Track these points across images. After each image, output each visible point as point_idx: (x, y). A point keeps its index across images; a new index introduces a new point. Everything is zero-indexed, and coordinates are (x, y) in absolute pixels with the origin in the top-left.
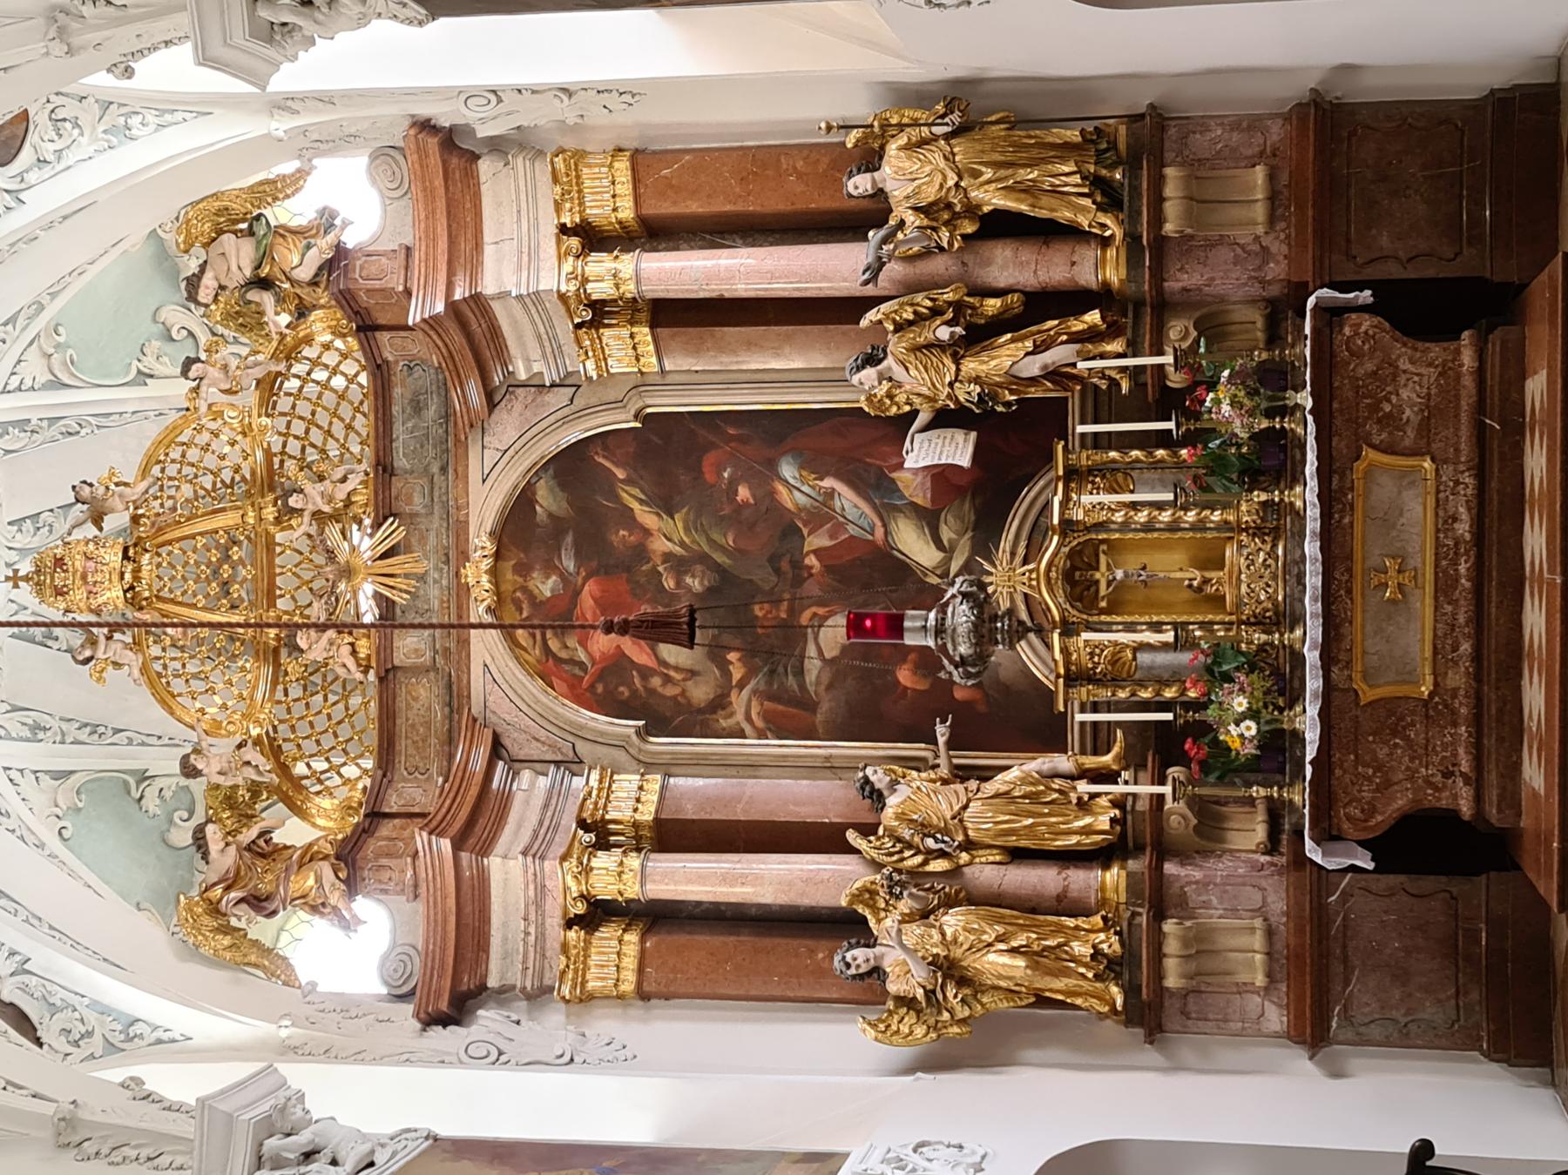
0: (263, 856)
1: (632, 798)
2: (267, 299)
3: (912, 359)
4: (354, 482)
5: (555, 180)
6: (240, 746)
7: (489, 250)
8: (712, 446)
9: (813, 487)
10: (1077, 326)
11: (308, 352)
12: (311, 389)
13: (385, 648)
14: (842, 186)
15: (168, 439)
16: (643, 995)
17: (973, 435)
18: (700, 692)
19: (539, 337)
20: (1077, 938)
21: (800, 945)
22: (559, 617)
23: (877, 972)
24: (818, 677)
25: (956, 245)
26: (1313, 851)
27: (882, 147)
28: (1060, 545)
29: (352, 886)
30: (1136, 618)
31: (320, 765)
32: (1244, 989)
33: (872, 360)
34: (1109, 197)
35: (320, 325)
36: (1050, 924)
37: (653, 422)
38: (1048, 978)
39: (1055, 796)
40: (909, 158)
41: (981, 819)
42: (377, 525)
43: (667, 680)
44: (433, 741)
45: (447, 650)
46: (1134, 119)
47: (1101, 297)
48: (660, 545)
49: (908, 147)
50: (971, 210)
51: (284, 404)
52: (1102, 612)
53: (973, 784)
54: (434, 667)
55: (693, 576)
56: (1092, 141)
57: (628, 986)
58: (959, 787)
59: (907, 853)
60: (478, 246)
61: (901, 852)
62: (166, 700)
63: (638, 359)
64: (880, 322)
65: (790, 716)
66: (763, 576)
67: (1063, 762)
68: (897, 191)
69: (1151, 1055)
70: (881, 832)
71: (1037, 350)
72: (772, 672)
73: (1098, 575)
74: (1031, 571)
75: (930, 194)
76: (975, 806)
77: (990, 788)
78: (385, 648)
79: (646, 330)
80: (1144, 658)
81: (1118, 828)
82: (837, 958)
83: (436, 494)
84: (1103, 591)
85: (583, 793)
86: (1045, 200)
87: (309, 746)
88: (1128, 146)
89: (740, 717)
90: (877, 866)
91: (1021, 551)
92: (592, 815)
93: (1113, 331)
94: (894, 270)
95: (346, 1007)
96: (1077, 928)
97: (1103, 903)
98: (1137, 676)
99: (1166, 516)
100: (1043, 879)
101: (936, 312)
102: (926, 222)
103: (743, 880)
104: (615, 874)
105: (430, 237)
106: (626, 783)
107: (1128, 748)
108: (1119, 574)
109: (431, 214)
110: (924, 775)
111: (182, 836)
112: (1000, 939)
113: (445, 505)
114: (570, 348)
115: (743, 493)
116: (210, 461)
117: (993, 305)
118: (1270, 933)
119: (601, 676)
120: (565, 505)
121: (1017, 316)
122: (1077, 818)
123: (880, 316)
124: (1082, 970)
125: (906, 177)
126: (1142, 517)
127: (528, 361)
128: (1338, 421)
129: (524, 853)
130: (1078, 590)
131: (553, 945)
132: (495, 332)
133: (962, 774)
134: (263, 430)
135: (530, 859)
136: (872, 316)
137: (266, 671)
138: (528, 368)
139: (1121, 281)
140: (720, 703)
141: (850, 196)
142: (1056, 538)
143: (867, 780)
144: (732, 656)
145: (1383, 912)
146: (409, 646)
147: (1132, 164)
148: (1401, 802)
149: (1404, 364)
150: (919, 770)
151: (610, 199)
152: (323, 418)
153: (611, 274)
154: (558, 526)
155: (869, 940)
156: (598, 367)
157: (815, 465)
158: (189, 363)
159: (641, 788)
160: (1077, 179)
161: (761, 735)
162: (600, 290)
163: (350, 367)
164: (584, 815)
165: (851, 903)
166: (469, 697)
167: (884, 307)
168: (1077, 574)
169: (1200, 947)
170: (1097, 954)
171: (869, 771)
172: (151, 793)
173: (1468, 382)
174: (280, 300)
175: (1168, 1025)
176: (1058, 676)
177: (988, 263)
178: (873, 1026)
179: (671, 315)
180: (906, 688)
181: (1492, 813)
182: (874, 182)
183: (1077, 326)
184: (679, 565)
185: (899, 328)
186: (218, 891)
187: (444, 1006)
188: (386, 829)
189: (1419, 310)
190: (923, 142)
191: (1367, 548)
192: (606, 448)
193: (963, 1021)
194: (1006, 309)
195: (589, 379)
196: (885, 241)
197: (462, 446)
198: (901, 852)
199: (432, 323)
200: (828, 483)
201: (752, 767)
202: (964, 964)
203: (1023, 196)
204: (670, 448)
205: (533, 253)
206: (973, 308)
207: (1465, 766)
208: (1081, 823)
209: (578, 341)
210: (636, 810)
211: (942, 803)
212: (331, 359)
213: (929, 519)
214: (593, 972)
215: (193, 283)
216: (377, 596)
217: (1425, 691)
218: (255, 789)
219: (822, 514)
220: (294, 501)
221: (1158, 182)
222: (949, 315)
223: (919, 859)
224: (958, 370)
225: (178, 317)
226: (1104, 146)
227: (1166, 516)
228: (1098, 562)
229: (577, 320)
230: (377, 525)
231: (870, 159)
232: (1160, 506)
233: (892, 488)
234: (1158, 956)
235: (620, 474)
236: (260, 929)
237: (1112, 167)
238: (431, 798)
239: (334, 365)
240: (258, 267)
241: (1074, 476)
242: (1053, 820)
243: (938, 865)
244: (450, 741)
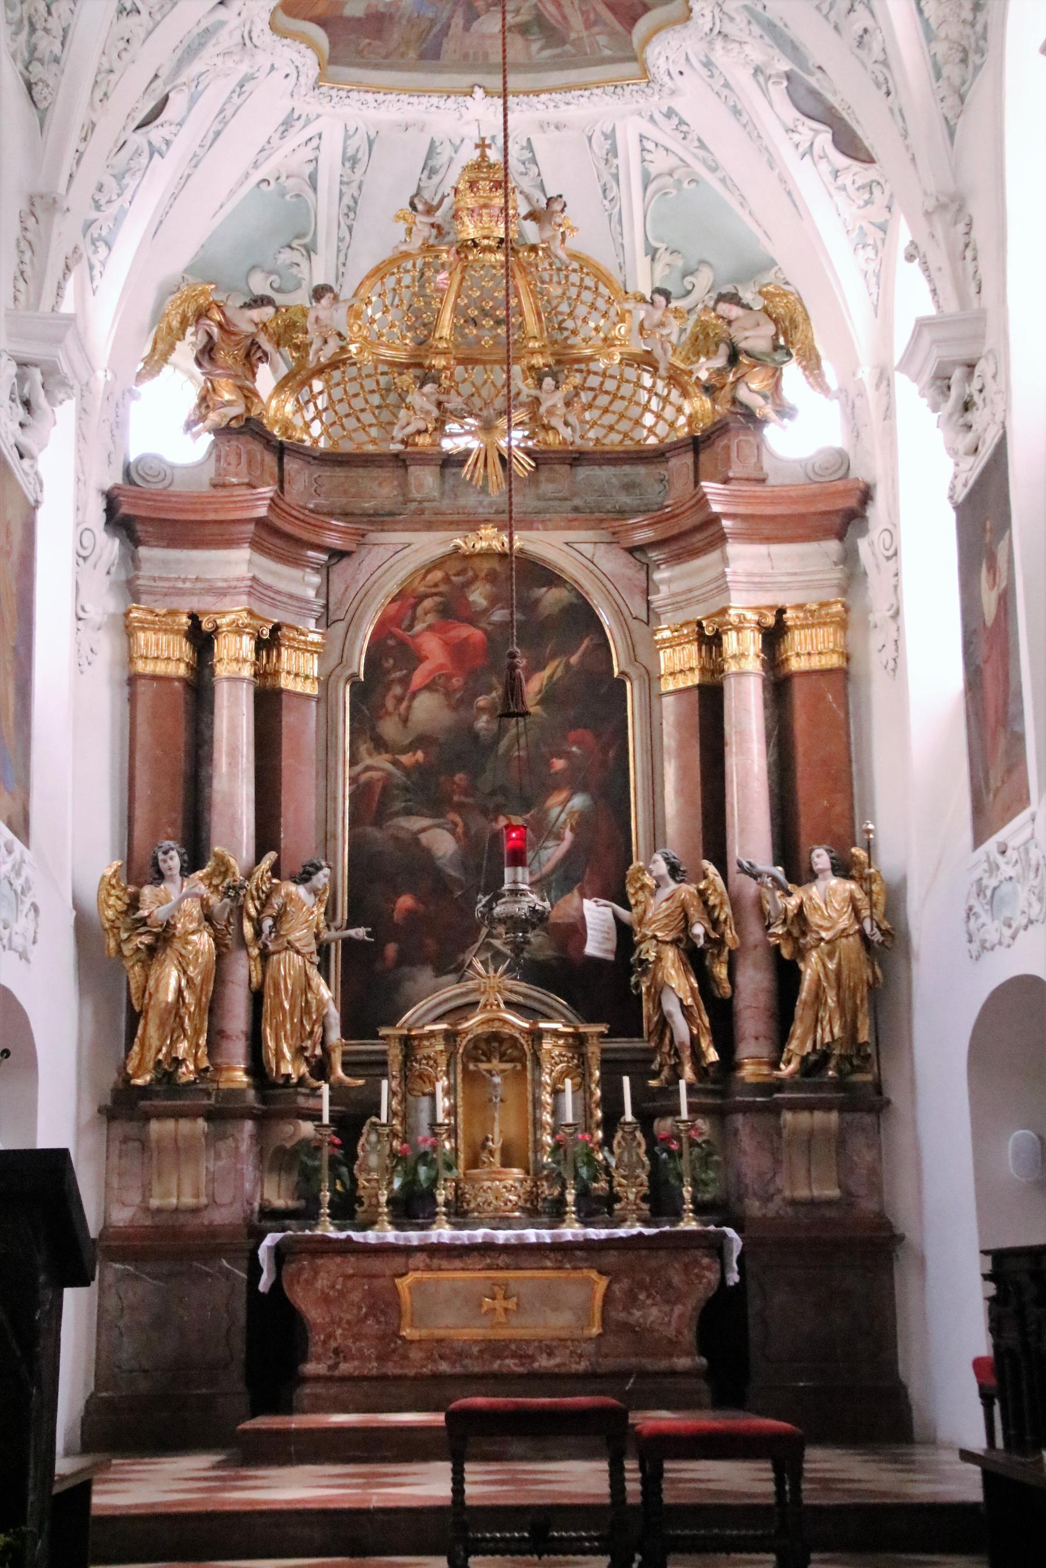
0: (248, 355)
1: (299, 671)
2: (720, 361)
3: (675, 904)
4: (566, 433)
5: (822, 605)
6: (340, 335)
7: (762, 549)
8: (598, 736)
9: (565, 822)
10: (705, 1042)
11: (675, 395)
12: (644, 396)
14: (819, 844)
15: (601, 276)
16: (133, 680)
17: (611, 957)
18: (389, 728)
19: (690, 590)
20: (190, 1047)
21: (178, 817)
22: (452, 610)
23: (159, 877)
24: (402, 828)
25: (772, 939)
26: (270, 1240)
27: (852, 878)
28: (522, 1030)
29: (223, 432)
30: (460, 1094)
31: (321, 402)
32: (146, 1191)
33: (674, 870)
34: (813, 1066)
35: (699, 404)
36: (202, 1023)
37: (619, 687)
38: (157, 1021)
39: (308, 1028)
40: (844, 900)
41: (289, 966)
42: (528, 452)
43: (399, 700)
44: (344, 500)
45: (422, 512)
46: (878, 1087)
47: (729, 1062)
49: (852, 900)
50: (801, 952)
51: (631, 373)
52: (465, 1069)
53: (316, 959)
54: (407, 501)
55: (488, 722)
56: (859, 1051)
57: (141, 667)
58: (314, 947)
59: (257, 903)
60: (768, 540)
61: (259, 898)
62: (379, 272)
63: (672, 674)
64: (706, 877)
65: (370, 805)
66: (487, 781)
67: (335, 1035)
68: (815, 891)
69: (90, 1110)
70: (275, 881)
71: (685, 1009)
72: (406, 789)
73: (495, 1061)
74: (498, 1005)
75: (814, 919)
76: (298, 960)
77: (313, 972)
78: (423, 459)
79: (696, 681)
80: (425, 1102)
81: (281, 1081)
82: (171, 843)
83: (556, 503)
84: (483, 1066)
85: (293, 628)
86: (809, 1015)
87: (337, 393)
88: (854, 1084)
89: (368, 761)
90: (249, 876)
91: (515, 998)
92: (284, 636)
93: (701, 1071)
94: (751, 887)
95: (118, 425)
96: (198, 1046)
97: (218, 1069)
98: (410, 1098)
99: (547, 1118)
100: (237, 1018)
101: (715, 923)
102: (790, 914)
103: (233, 763)
104: (235, 654)
105: (774, 500)
106: (312, 665)
107: (349, 1088)
108: (497, 1080)
109: (794, 501)
110: (322, 917)
111: (259, 285)
112: (190, 981)
113: (545, 511)
114: (682, 617)
115: (559, 764)
116: (582, 310)
117: (721, 971)
118: (195, 1211)
119: (402, 643)
120: (547, 613)
121: (712, 992)
122: (290, 1046)
123: (711, 876)
124: (164, 1050)
125: (827, 897)
126: (547, 1098)
127: (669, 581)
128: (631, 1255)
129: (254, 579)
130: (483, 1046)
131: (176, 603)
132: (695, 553)
133: (323, 950)
134: (610, 356)
135: (249, 583)
136: (711, 869)
137: (402, 357)
138: (663, 581)
139: (743, 1078)
140: (380, 744)
141: (812, 851)
142: (527, 1025)
143: (319, 868)
144: (420, 755)
145: (216, 1303)
146: (425, 480)
147: (840, 1084)
148: (313, 1313)
149: (678, 1309)
150: (326, 913)
151: (808, 651)
152: (619, 406)
153: (744, 650)
154: (529, 606)
156: (664, 641)
157: (583, 824)
158: (666, 294)
159: (307, 677)
160: (828, 1039)
161: (353, 780)
162: (731, 642)
163: (662, 429)
164: (284, 630)
165: (216, 855)
166: (382, 530)
167: (719, 880)
168: (496, 1044)
169: (181, 1151)
170: (178, 1062)
171: (326, 871)
172: (296, 257)
173: (663, 1364)
174: (720, 372)
175: (116, 1125)
176: (409, 1030)
177: (755, 965)
178: (114, 875)
179: (710, 699)
180: (395, 903)
181: (307, 1390)
182: (823, 871)
183: (705, 1042)
185: (702, 893)
186: (218, 317)
187: (124, 510)
188: (270, 460)
189: (722, 1321)
190: (856, 911)
191: (525, 1278)
192: (597, 646)
193: (119, 951)
194: (718, 985)
195: (654, 633)
196: (775, 879)
197: (598, 524)
198: (259, 898)
199: (702, 501)
200: (568, 835)
201: (327, 772)
202: (168, 951)
203: (813, 994)
204: (598, 701)
205: (760, 586)
206: (719, 955)
207: (345, 1368)
208: (286, 1050)
209: (686, 624)
210: (289, 673)
211: (300, 934)
212: (669, 413)
214: (151, 636)
215: (733, 299)
216: (467, 453)
217: (406, 1332)
218: (302, 348)
219: (544, 831)
220: (548, 382)
221: (826, 1106)
222: (714, 935)
223: (253, 912)
224: (666, 943)
225: (703, 280)
226: (855, 1062)
227: (547, 1118)
228: (506, 1061)
229: (704, 623)
230: (528, 452)
231: (843, 868)
232: (556, 1112)
233: (565, 890)
234: (177, 1115)
235: (574, 660)
236: (185, 351)
237: (839, 1071)
238: (295, 495)
239: (662, 416)
240: (748, 354)
241: (578, 1041)
242: (288, 1026)
243: (248, 928)
244: (345, 515)
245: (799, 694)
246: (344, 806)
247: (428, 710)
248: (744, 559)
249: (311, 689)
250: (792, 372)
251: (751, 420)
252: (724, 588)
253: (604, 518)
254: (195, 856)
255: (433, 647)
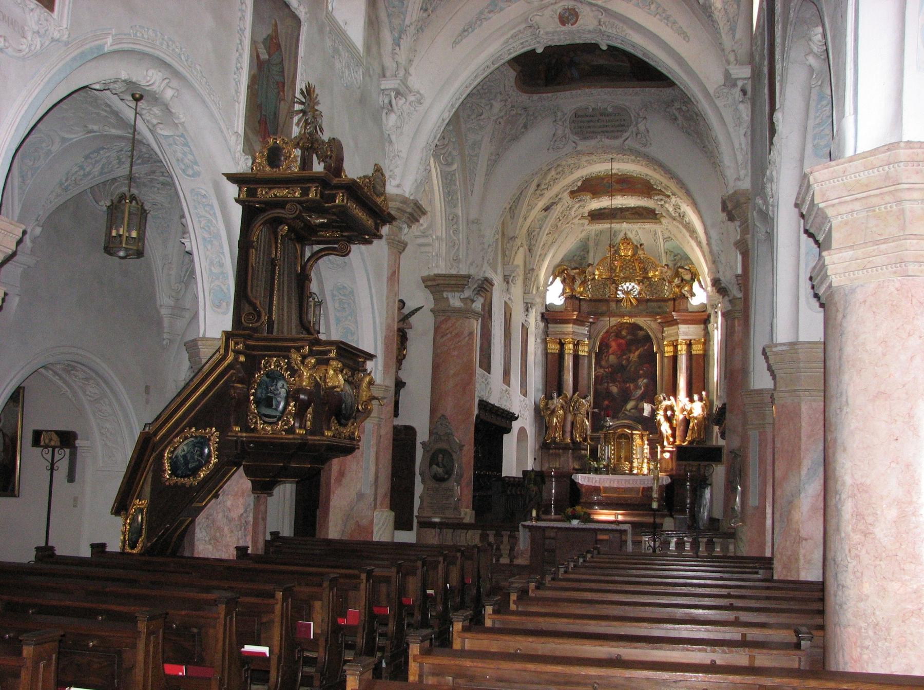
1: (584, 351)
13: (613, 301)
22: (618, 335)
29: (566, 298)
48: (632, 356)
62: (602, 260)
95: (544, 298)
104: (569, 348)
133: (588, 414)
140: (601, 367)
146: (613, 305)
153: (682, 349)
155: (558, 397)
157: (646, 386)
162: (679, 347)
169: (558, 455)
179: (675, 359)
184: (628, 359)
188: (577, 302)
204: (650, 358)
211: (583, 411)
213: (636, 407)
215: (682, 268)
239: (667, 291)
245: (694, 358)
246: (593, 380)
247: (612, 359)
248: (683, 328)
249: (586, 354)
250: (696, 285)
251: (684, 297)
252: (677, 335)
253: (652, 314)
254: (560, 394)
255: (613, 344)
